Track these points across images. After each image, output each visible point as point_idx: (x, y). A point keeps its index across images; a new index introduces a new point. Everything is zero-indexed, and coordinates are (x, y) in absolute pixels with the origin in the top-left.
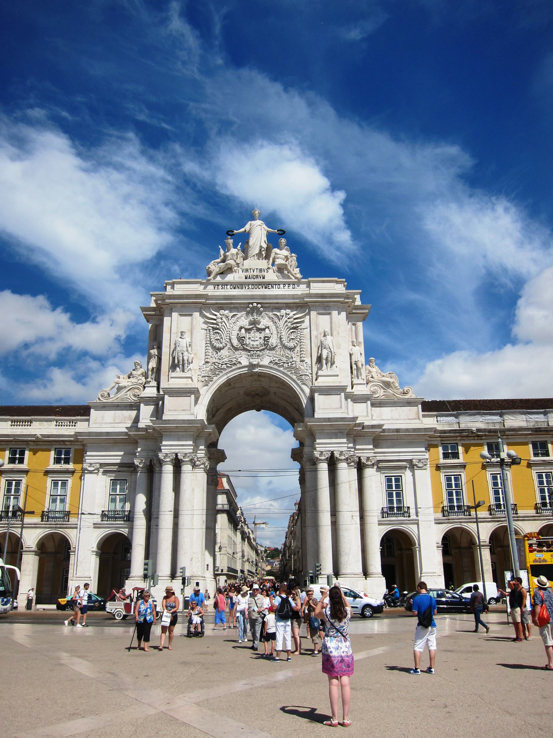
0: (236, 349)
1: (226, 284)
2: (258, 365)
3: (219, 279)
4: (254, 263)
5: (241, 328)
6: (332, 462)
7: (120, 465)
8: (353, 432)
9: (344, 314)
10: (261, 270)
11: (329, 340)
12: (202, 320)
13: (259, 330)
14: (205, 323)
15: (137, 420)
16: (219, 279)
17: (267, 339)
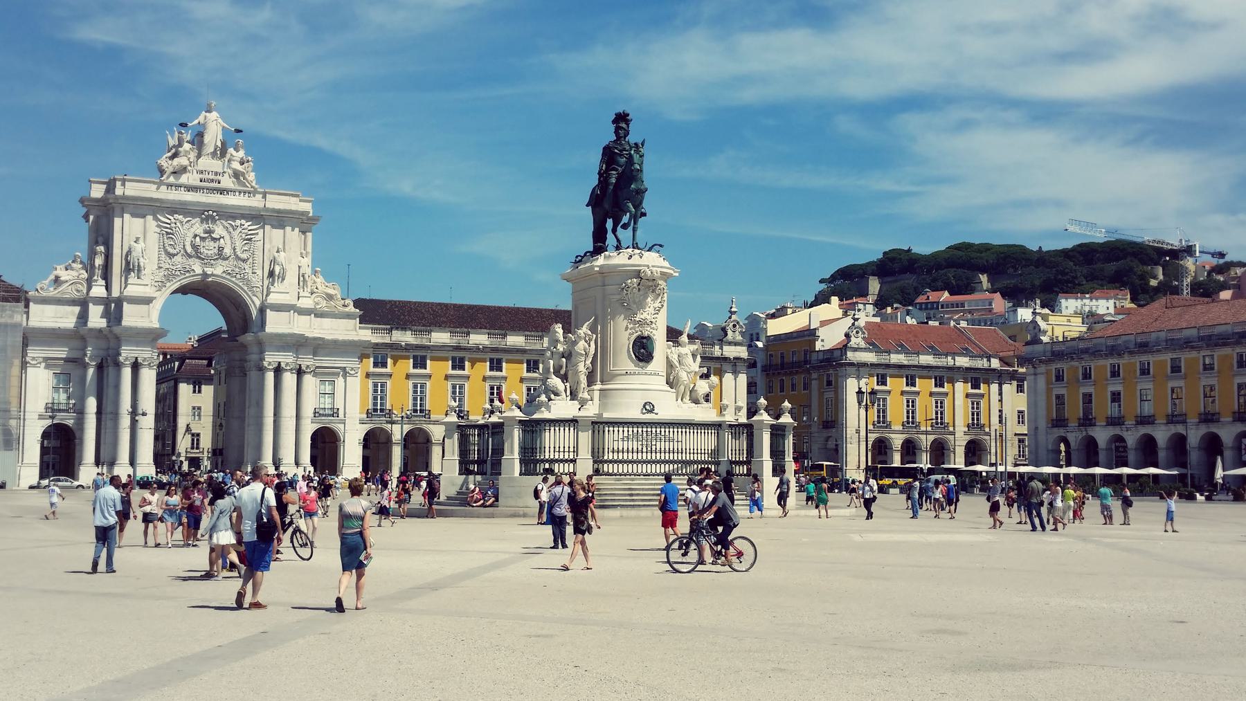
0: (190, 256)
1: (178, 186)
2: (213, 275)
3: (172, 179)
4: (207, 163)
5: (196, 236)
6: (278, 371)
7: (67, 360)
8: (298, 344)
9: (297, 230)
10: (216, 174)
11: (281, 257)
12: (155, 223)
13: (214, 240)
14: (158, 226)
15: (83, 317)
16: (172, 179)
17: (221, 249)
